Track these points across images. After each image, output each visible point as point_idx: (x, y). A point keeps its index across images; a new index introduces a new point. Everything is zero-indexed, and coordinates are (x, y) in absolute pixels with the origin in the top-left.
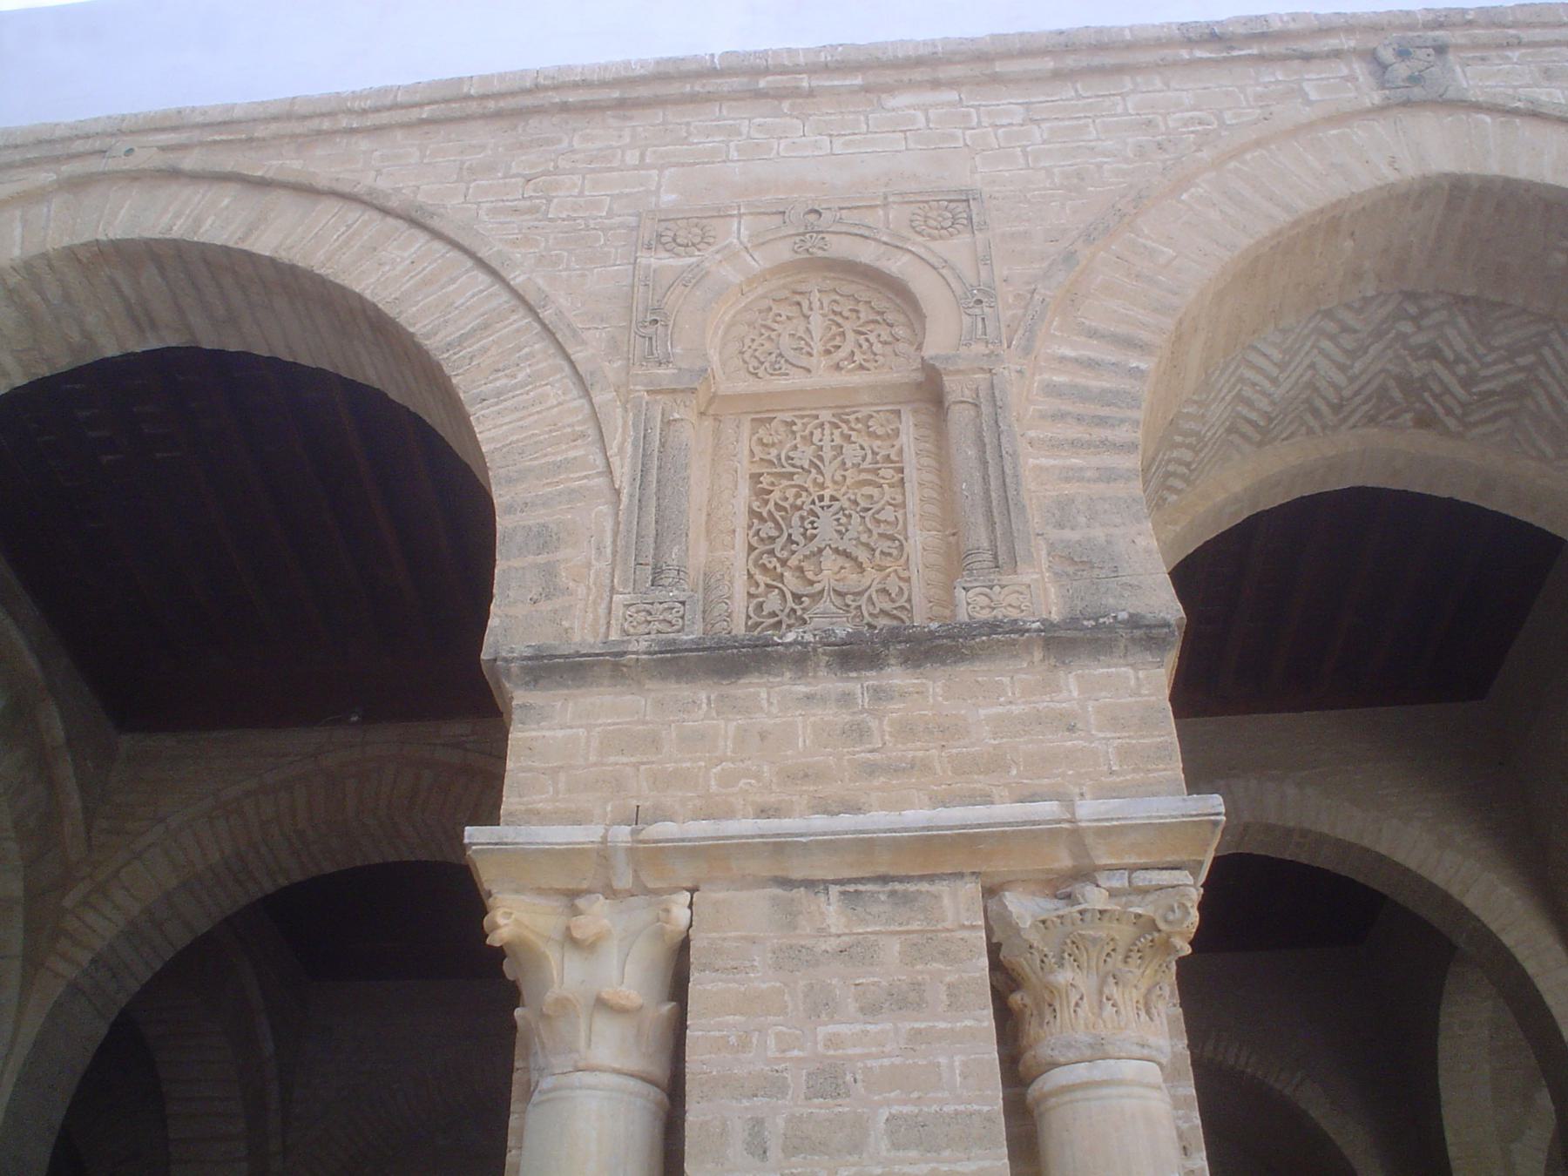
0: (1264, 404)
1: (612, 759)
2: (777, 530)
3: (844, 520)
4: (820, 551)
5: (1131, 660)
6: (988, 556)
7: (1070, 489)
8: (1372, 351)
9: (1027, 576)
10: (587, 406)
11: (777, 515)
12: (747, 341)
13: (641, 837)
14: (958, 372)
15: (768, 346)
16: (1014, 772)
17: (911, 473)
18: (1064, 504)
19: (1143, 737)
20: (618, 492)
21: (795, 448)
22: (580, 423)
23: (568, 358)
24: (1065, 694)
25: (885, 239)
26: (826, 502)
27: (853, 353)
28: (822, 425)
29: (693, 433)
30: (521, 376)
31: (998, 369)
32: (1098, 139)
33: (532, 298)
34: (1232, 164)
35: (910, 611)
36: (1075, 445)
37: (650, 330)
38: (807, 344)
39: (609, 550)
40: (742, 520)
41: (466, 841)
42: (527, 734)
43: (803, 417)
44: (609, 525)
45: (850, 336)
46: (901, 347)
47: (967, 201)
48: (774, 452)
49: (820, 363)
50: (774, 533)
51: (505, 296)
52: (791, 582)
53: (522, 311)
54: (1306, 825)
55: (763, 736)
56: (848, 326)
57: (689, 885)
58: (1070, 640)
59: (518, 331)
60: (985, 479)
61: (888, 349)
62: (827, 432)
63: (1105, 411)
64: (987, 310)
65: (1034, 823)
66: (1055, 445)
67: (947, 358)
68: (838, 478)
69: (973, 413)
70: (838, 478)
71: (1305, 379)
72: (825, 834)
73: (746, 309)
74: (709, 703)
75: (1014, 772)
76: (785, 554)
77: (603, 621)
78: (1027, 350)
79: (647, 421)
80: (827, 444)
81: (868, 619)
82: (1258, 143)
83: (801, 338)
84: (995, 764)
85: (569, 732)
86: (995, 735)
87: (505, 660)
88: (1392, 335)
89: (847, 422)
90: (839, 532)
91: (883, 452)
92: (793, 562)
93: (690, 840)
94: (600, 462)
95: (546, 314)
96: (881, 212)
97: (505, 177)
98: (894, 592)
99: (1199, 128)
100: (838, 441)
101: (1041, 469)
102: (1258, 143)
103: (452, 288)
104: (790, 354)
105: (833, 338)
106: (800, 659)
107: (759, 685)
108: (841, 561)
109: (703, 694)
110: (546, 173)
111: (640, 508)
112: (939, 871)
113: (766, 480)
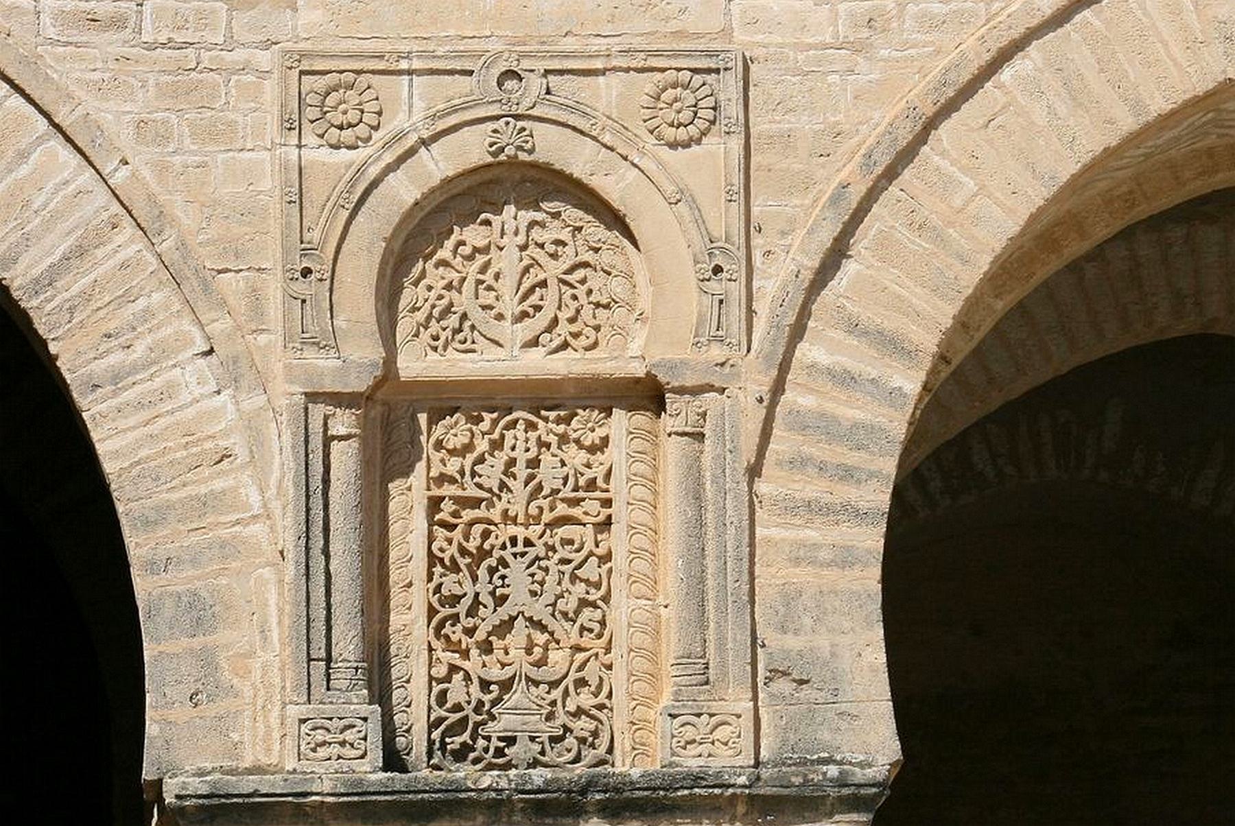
26: (520, 548)
30: (139, 350)
103: (24, 170)
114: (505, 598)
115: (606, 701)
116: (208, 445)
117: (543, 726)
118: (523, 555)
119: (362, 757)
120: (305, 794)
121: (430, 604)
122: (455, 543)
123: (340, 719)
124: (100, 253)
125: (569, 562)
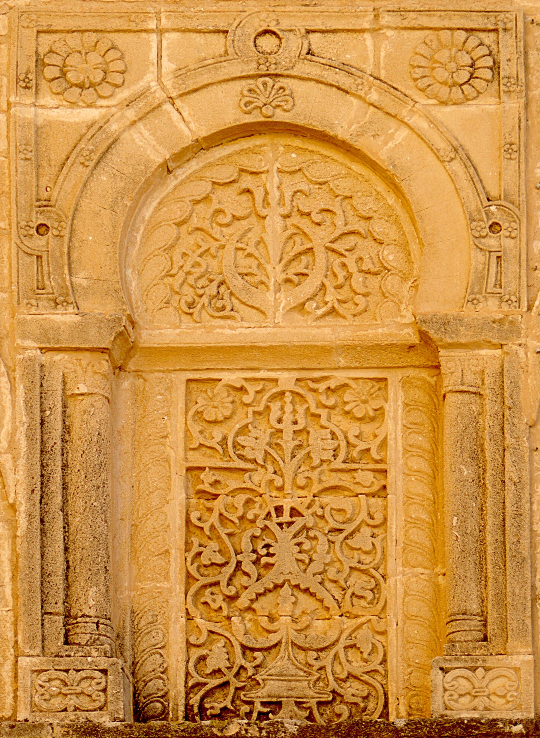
17: (396, 480)
26: (286, 517)
35: (386, 676)
48: (218, 433)
62: (288, 408)
80: (287, 427)
81: (333, 685)
98: (366, 649)
114: (268, 566)
115: (380, 668)
117: (311, 693)
118: (290, 524)
119: (101, 709)
121: (188, 572)
122: (216, 514)
123: (78, 671)
125: (340, 531)
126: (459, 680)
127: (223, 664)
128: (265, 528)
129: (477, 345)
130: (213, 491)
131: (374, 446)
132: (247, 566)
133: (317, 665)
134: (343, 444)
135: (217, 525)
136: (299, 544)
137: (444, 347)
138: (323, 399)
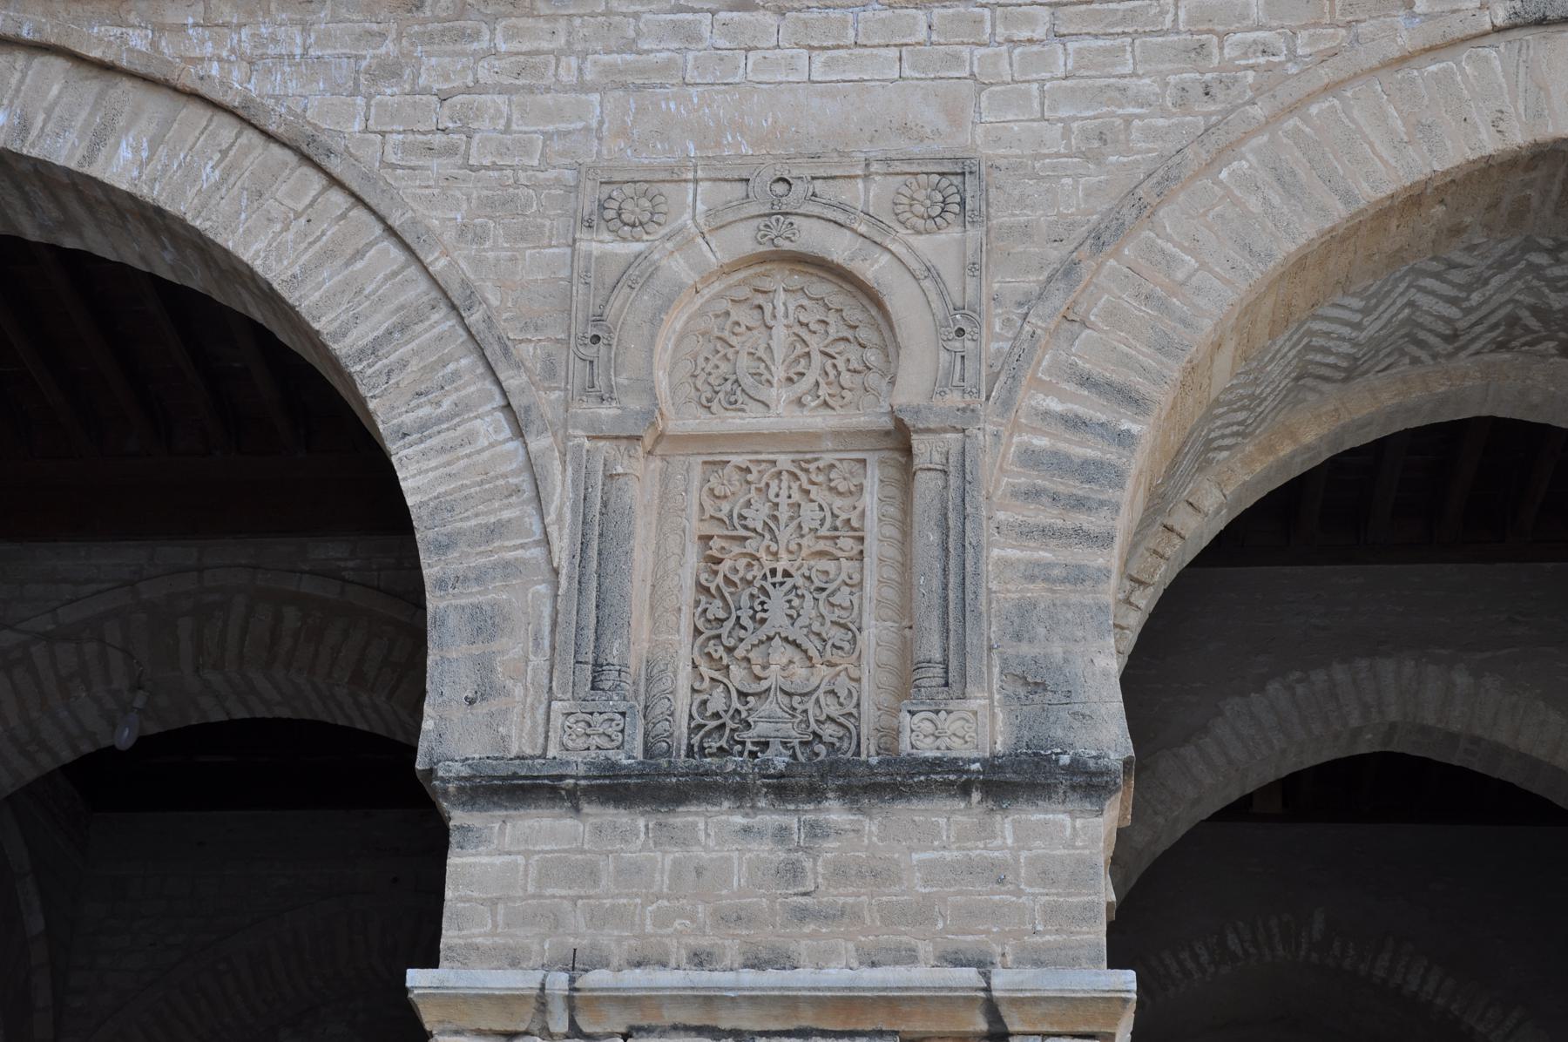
0: (1346, 348)
1: (549, 892)
2: (729, 612)
3: (796, 602)
4: (770, 639)
5: (1069, 806)
6: (938, 670)
7: (1036, 590)
8: (1495, 282)
9: (977, 702)
10: (521, 451)
11: (726, 591)
12: (701, 360)
13: (577, 985)
14: (928, 430)
15: (724, 368)
16: (940, 925)
17: (872, 547)
18: (1025, 609)
19: (1070, 895)
20: (556, 572)
21: (748, 504)
22: (515, 473)
23: (498, 383)
24: (999, 842)
25: (863, 229)
26: (779, 578)
27: (817, 384)
28: (780, 473)
29: (641, 478)
30: (447, 404)
31: (972, 431)
32: (1134, 74)
33: (456, 294)
34: (1293, 122)
35: (858, 719)
36: (1047, 533)
37: (590, 351)
38: (767, 367)
39: (547, 643)
40: (689, 594)
41: (408, 984)
42: (464, 860)
43: (759, 462)
44: (547, 611)
45: (817, 359)
46: (872, 379)
47: (963, 174)
48: (726, 507)
49: (779, 395)
50: (722, 615)
51: (423, 284)
52: (738, 674)
53: (444, 309)
54: (1478, 732)
55: (699, 872)
56: (815, 343)
57: (623, 1030)
58: (1011, 780)
59: (440, 338)
60: (945, 570)
61: (858, 378)
62: (784, 485)
63: (1082, 490)
64: (969, 344)
65: (951, 989)
66: (1026, 533)
67: (917, 412)
68: (793, 547)
69: (940, 483)
70: (793, 547)
71: (1401, 316)
72: (753, 989)
73: (701, 312)
74: (647, 833)
75: (940, 925)
76: (732, 642)
77: (541, 729)
78: (1007, 404)
79: (588, 475)
80: (783, 501)
81: (814, 726)
82: (1330, 89)
83: (760, 359)
84: (921, 914)
85: (507, 858)
86: (926, 883)
87: (442, 779)
88: (1522, 265)
89: (807, 471)
90: (791, 616)
91: (844, 516)
92: (740, 653)
93: (624, 989)
94: (537, 528)
95: (474, 318)
96: (860, 184)
97: (413, 93)
98: (843, 694)
99: (1262, 60)
100: (796, 497)
101: (1006, 563)
102: (1330, 89)
103: (359, 265)
104: (747, 381)
105: (797, 360)
106: (740, 792)
107: (697, 814)
108: (790, 649)
109: (637, 821)
110: (468, 90)
111: (580, 592)
112: (860, 1028)
113: (716, 544)
114: (763, 621)
115: (855, 712)
116: (501, 482)
117: (794, 733)
118: (782, 584)
120: (562, 777)
122: (721, 576)
124: (418, 328)
125: (823, 590)
126: (922, 722)
127: (721, 707)
128: (763, 589)
129: (945, 431)
130: (719, 556)
131: (854, 517)
132: (745, 621)
133: (800, 708)
134: (828, 515)
135: (722, 585)
136: (789, 601)
137: (916, 432)
138: (813, 477)
